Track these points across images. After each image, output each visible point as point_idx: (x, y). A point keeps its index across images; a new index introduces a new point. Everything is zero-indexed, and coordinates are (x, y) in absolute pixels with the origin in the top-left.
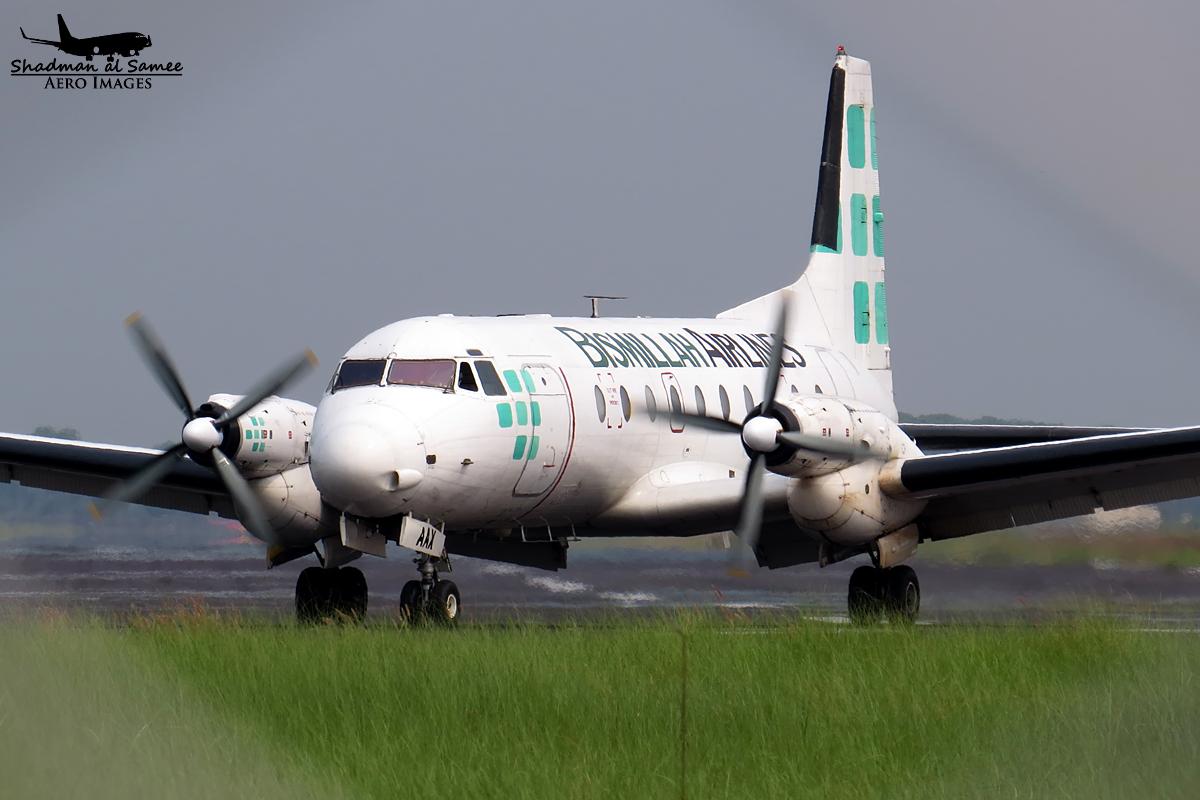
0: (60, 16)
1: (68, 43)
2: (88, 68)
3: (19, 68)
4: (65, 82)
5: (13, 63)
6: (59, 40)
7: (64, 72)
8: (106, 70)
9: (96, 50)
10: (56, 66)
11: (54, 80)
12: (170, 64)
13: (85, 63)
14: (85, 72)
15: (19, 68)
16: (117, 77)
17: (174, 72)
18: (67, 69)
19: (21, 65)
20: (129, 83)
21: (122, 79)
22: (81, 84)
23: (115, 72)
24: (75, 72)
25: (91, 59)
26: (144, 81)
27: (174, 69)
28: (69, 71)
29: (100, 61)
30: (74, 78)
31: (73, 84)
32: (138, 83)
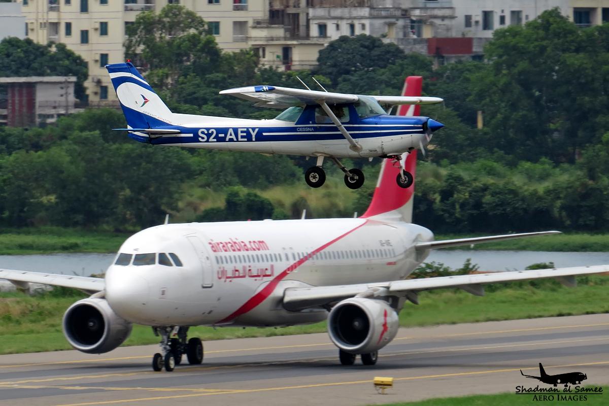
0: (540, 364)
2: (555, 390)
4: (543, 397)
5: (516, 388)
10: (539, 389)
17: (598, 392)
20: (575, 398)
21: (572, 396)
22: (551, 398)
23: (568, 392)
24: (548, 392)
29: (561, 387)
30: (548, 396)
31: (547, 398)
32: (580, 398)
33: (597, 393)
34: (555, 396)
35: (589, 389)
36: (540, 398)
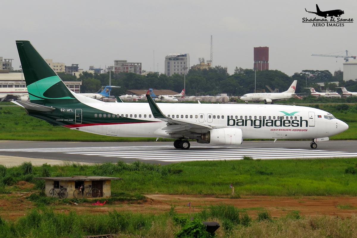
0: (317, 5)
1: (319, 13)
2: (325, 20)
3: (305, 20)
4: (318, 24)
5: (303, 19)
6: (317, 12)
7: (318, 21)
8: (331, 21)
10: (316, 20)
11: (315, 24)
12: (350, 19)
13: (324, 19)
14: (324, 21)
15: (305, 20)
17: (351, 21)
18: (319, 21)
19: (305, 19)
20: (337, 25)
21: (335, 24)
22: (323, 25)
23: (333, 21)
24: (321, 21)
26: (342, 24)
27: (351, 20)
28: (320, 21)
29: (329, 18)
30: (321, 23)
31: (321, 25)
32: (340, 25)
35: (345, 19)
36: (316, 25)
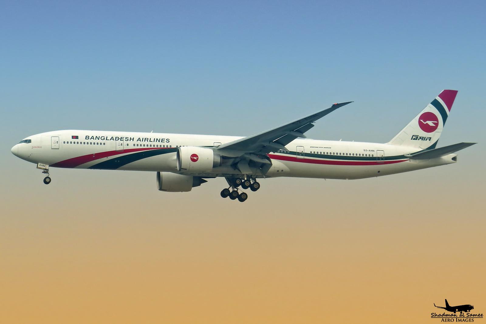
0: (446, 300)
1: (448, 308)
2: (454, 315)
3: (434, 316)
5: (432, 314)
6: (446, 307)
7: (447, 317)
8: (460, 316)
9: (457, 310)
11: (444, 319)
12: (480, 314)
14: (453, 317)
15: (434, 316)
16: (463, 318)
17: (481, 317)
18: (448, 316)
19: (434, 315)
20: (467, 320)
21: (465, 319)
22: (452, 320)
23: (463, 317)
24: (450, 317)
25: (455, 313)
26: (471, 319)
27: (480, 316)
28: (449, 317)
29: (458, 313)
30: (450, 319)
31: (450, 320)
32: (470, 320)
33: (480, 317)
34: (455, 319)
35: (475, 315)
36: (446, 320)
